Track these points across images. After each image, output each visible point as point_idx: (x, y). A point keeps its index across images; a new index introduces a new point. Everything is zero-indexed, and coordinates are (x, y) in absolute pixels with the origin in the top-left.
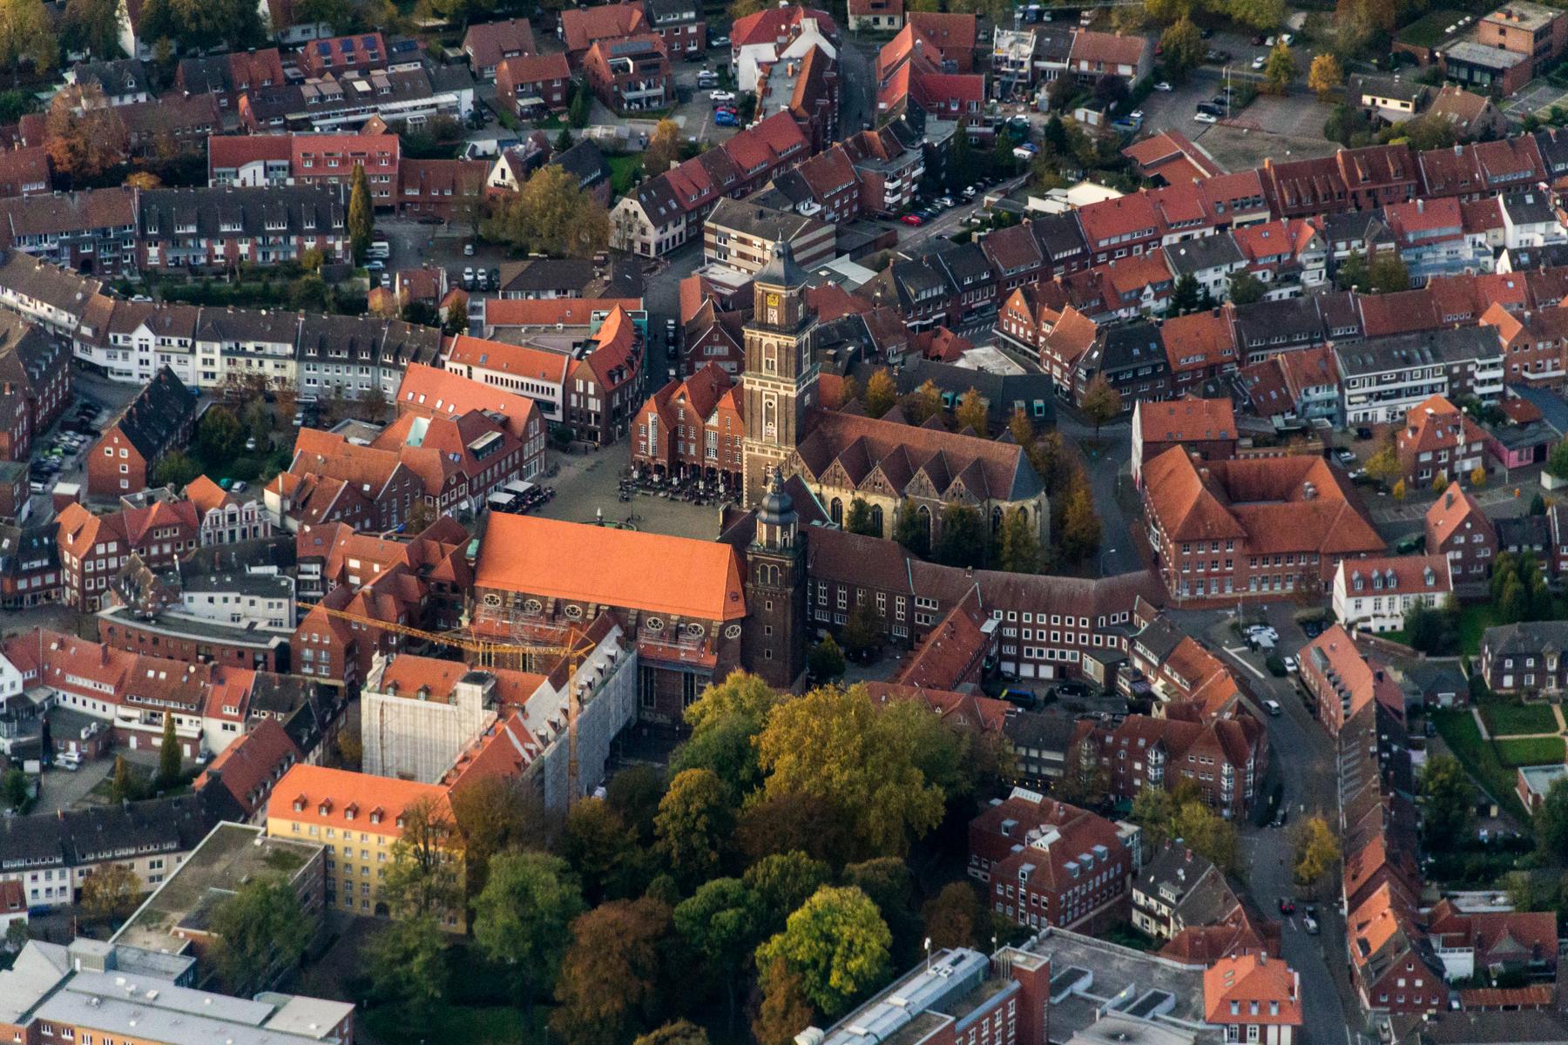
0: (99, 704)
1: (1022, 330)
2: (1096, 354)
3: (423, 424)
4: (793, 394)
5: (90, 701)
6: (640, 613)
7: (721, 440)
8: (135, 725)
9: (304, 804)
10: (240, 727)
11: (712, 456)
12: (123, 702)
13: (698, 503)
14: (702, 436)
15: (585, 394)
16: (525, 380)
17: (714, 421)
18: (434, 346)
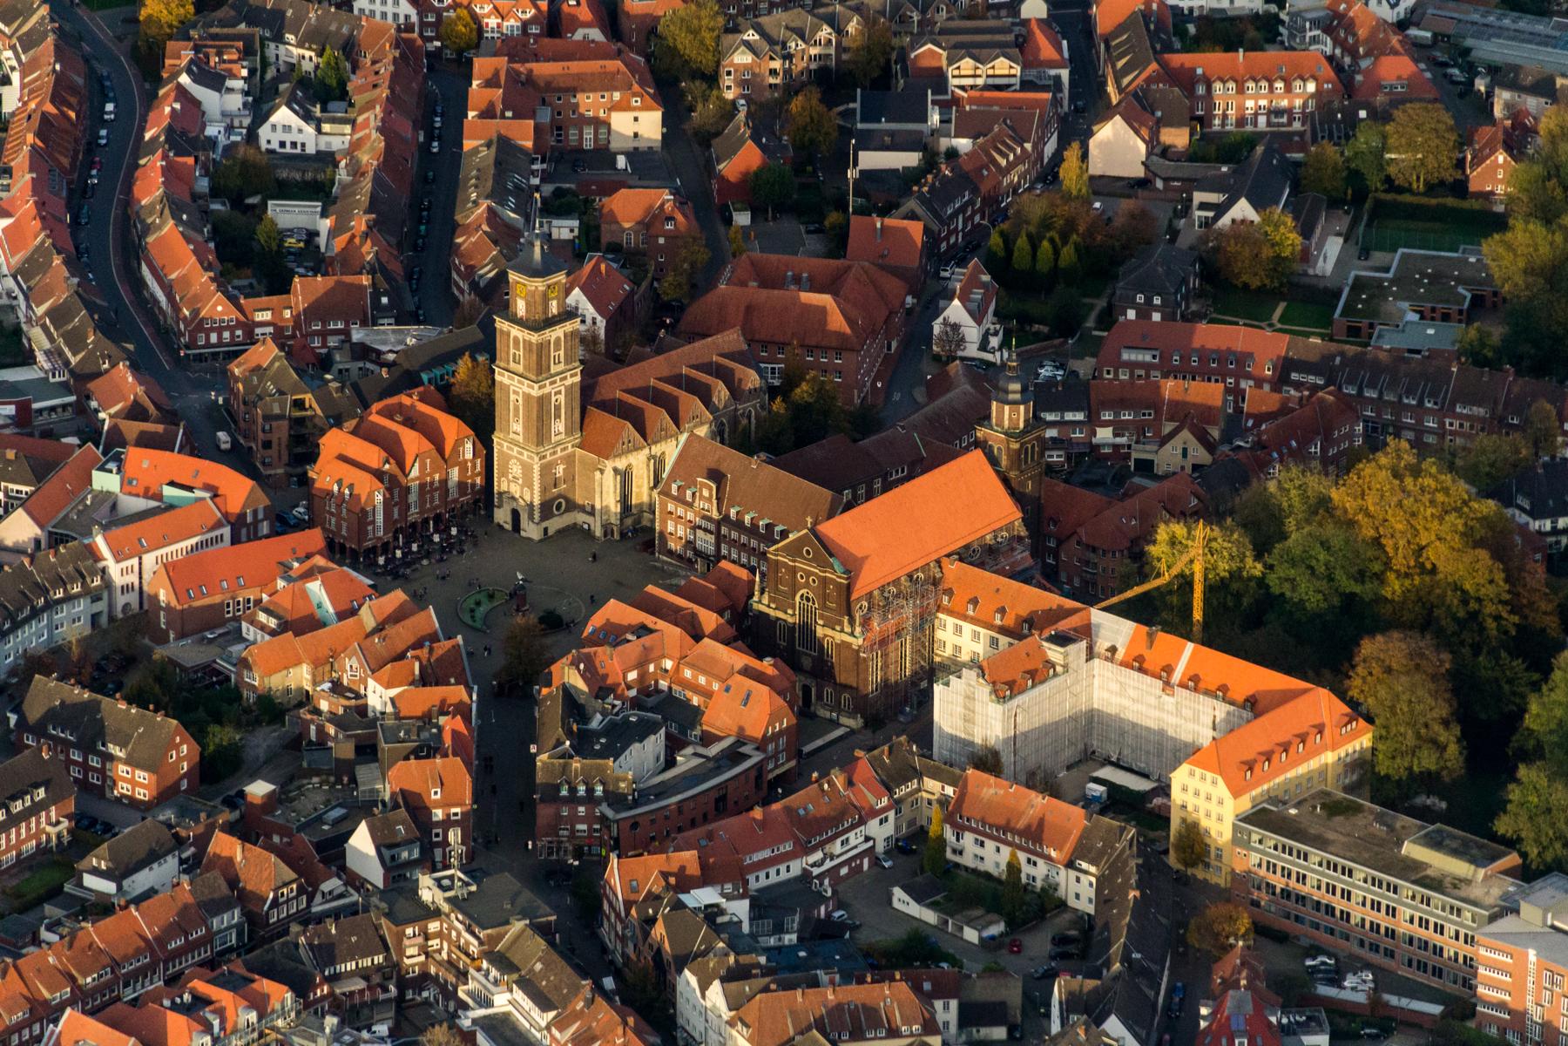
0: (783, 868)
1: (226, 335)
2: (385, 300)
3: (315, 588)
4: (578, 379)
5: (772, 871)
6: (967, 547)
7: (422, 486)
8: (828, 864)
9: (1250, 766)
10: (891, 814)
11: (413, 510)
12: (809, 851)
13: (461, 552)
14: (408, 489)
15: (256, 522)
16: (194, 541)
17: (415, 473)
18: (85, 559)
